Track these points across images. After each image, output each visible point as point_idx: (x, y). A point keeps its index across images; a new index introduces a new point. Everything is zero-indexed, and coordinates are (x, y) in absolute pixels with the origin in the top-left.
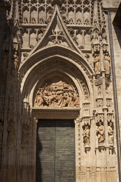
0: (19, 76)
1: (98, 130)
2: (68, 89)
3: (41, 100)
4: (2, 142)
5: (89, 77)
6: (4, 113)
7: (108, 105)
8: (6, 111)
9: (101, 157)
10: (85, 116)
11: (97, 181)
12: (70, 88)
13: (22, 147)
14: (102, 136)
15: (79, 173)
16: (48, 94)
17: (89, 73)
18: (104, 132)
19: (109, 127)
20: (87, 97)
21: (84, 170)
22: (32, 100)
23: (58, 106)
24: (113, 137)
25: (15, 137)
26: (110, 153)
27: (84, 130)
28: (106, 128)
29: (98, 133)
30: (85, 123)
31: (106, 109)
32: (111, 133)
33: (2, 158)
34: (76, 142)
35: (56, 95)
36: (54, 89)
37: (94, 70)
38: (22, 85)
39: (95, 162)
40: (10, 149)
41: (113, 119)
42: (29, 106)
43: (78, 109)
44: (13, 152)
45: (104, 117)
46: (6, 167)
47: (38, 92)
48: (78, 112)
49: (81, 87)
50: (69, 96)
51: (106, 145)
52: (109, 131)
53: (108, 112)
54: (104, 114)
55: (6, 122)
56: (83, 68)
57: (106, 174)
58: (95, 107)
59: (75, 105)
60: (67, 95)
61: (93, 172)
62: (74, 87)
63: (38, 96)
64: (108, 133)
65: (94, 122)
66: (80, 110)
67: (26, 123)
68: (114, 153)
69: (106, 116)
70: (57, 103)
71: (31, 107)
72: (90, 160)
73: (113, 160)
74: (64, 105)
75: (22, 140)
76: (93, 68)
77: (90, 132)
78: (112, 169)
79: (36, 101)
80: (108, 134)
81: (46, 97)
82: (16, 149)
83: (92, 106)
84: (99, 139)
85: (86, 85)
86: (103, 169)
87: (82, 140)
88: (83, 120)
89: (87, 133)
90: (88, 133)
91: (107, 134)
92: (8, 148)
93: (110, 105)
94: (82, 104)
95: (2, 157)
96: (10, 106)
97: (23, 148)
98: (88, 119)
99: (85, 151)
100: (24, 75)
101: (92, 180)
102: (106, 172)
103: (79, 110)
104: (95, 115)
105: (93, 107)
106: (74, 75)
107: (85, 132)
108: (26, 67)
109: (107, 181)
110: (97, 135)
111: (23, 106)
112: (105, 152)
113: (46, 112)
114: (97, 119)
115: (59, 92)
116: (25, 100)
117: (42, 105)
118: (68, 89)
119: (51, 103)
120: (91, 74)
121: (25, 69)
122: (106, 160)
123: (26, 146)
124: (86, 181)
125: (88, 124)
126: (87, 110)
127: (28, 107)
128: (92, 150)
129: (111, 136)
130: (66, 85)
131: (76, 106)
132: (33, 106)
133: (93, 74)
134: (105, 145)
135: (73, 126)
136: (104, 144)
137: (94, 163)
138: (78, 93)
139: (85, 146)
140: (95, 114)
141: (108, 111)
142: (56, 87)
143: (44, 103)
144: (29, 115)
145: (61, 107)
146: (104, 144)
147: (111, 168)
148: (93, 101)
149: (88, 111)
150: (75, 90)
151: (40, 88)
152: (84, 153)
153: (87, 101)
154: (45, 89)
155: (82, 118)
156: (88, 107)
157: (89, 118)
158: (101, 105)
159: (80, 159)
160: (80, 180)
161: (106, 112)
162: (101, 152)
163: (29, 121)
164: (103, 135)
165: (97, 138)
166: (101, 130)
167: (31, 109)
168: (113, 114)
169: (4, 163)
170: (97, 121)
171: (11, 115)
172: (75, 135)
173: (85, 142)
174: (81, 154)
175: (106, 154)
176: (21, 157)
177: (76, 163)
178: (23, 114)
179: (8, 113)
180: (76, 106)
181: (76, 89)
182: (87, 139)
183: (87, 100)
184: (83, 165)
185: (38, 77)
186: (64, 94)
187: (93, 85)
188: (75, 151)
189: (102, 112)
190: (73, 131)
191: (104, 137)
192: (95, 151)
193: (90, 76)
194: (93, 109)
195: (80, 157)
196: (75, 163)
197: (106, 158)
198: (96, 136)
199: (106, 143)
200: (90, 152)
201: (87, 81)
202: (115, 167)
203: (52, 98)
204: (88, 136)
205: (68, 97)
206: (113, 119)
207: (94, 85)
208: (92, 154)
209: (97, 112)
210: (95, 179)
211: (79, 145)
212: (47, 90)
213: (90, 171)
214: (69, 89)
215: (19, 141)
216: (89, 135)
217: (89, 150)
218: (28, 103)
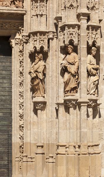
1: (64, 62)
7: (90, 6)
9: (69, 123)
10: (35, 29)
11: (59, 175)
14: (72, 78)
15: (19, 159)
18: (78, 68)
19: (90, 57)
21: (30, 151)
24: (98, 80)
26: (88, 116)
27: (34, 63)
28: (82, 59)
29: (64, 70)
30: (35, 47)
31: (84, 15)
32: (94, 72)
34: (13, 90)
39: (55, 135)
41: (99, 39)
43: (19, 11)
45: (79, 35)
48: (20, 18)
51: (81, 98)
52: (90, 67)
53: (89, 23)
54: (79, 27)
57: (79, 159)
58: (60, 9)
61: (51, 155)
64: (87, 71)
65: (56, 45)
66: (24, 14)
68: (98, 116)
69: (83, 32)
72: (45, 130)
73: (94, 131)
77: (47, 67)
78: (91, 150)
80: (86, 73)
83: (53, 8)
84: (66, 84)
86: (72, 149)
87: (28, 85)
88: (31, 40)
89: (39, 70)
90: (41, 69)
91: (83, 73)
93: (94, 7)
98: (43, 37)
99: (33, 111)
101: (48, 172)
102: (79, 155)
103: (23, 15)
104: (59, 29)
105: (55, 10)
107: (36, 67)
109: (79, 175)
110: (62, 74)
112: (78, 112)
114: (64, 38)
122: (78, 131)
124: (35, 175)
125: (42, 48)
126: (42, 15)
128: (51, 108)
129: (93, 79)
131: (14, 4)
134: (78, 98)
135: (8, 52)
136: (76, 94)
137: (54, 136)
139: (35, 100)
140: (60, 25)
141: (88, 20)
146: (76, 96)
147: (89, 146)
149: (43, 19)
152: (33, 113)
155: (30, 34)
156: (44, 8)
157: (44, 35)
158: (75, 5)
159: (21, 127)
160: (22, 174)
161: (84, 23)
162: (69, 113)
164: (76, 75)
165: (62, 80)
166: (70, 64)
168: (100, 27)
170: (64, 42)
172: (13, 74)
173: (34, 90)
174: (25, 117)
175: (81, 118)
177: (13, 138)
180: (14, 4)
182: (38, 84)
184: (29, 140)
188: (11, 109)
189: (75, 22)
190: (8, 64)
191: (78, 79)
192: (57, 111)
194: (55, 14)
195: (21, 123)
196: (10, 136)
197: (80, 125)
198: (61, 77)
199: (80, 94)
200: (45, 112)
202: (98, 145)
204: (41, 76)
206: (99, 39)
208: (50, 116)
209: (63, 20)
210: (55, 171)
211: (21, 96)
213: (43, 154)
216: (44, 75)
217: (43, 109)
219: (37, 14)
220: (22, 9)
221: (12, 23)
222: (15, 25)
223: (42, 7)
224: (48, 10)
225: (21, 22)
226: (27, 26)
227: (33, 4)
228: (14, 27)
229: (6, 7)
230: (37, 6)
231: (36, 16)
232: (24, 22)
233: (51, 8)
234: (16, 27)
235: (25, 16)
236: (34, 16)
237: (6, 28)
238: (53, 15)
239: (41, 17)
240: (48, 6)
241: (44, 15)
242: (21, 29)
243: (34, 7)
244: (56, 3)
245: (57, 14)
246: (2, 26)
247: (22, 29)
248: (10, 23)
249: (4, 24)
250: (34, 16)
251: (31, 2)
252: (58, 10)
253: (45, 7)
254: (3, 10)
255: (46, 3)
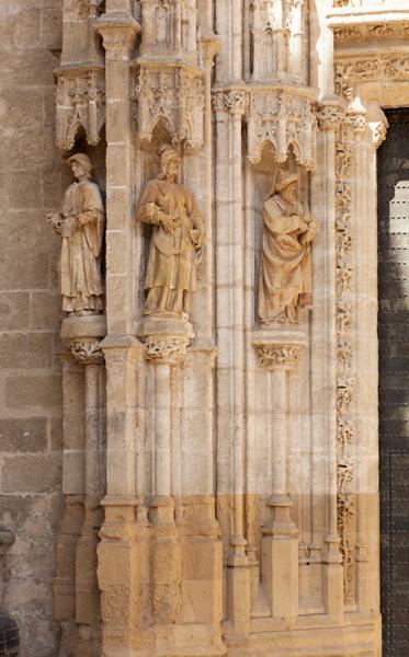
4: (102, 312)
6: (102, 73)
8: (118, 53)
13: (259, 349)
25: (200, 270)
33: (105, 443)
40: (164, 371)
44: (189, 393)
46: (143, 514)
55: (120, 151)
67: (284, 150)
75: (260, 288)
82: (216, 370)
92: (151, 360)
95: (110, 436)
96: (148, 12)
97: (265, 355)
123: (296, 336)
144: (309, 82)
163: (309, 129)
169: (125, 478)
171: (156, 91)
176: (256, 427)
179: (135, 71)
215: (236, 305)
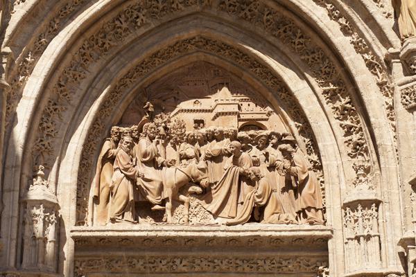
0: (9, 69)
2: (261, 127)
3: (125, 190)
5: (370, 66)
12: (276, 124)
16: (160, 160)
17: (371, 48)
20: (367, 171)
22: (74, 187)
23: (213, 221)
35: (202, 164)
36: (190, 131)
37: (396, 28)
38: (24, 110)
42: (60, 223)
47: (107, 145)
49: (333, 116)
50: (272, 168)
56: (336, 19)
59: (302, 213)
60: (256, 163)
62: (295, 119)
63: (107, 165)
66: (329, 237)
70: (209, 201)
71: (70, 226)
74: (245, 211)
76: (392, 21)
79: (93, 192)
81: (150, 172)
83: (393, 220)
85: (358, 106)
94: (338, 206)
100: (33, 64)
103: (325, 240)
105: (398, 223)
106: (296, 59)
108: (46, 22)
111: (24, 220)
113: (148, 254)
115: (214, 147)
116: (37, 191)
117: (128, 215)
118: (261, 127)
119: (176, 203)
120: (382, 52)
121: (37, 33)
126: (368, 238)
127: (51, 229)
130: (251, 110)
131: (305, 216)
132: (80, 221)
133: (391, 50)
138: (314, 147)
142: (199, 123)
143: (140, 206)
145: (229, 225)
148: (395, 190)
149: (374, 242)
150: (302, 132)
151: (115, 128)
153: (364, 192)
154: (140, 130)
167: (68, 235)
178: (24, 265)
180: (305, 216)
181: (307, 130)
183: (364, 186)
185: (104, 69)
186: (244, 155)
187: (391, 108)
193: (378, 58)
201: (360, 85)
203: (180, 176)
205: (263, 169)
207: (400, 108)
212: (151, 139)
214: (267, 132)
218: (52, 208)
219: (358, 234)
220: (323, 227)
221: (302, 258)
222: (309, 264)
223: (369, 220)
224: (381, 224)
225: (323, 256)
226: (337, 265)
227: (348, 213)
228: (308, 268)
229: (288, 224)
230: (356, 218)
231: (356, 241)
232: (330, 255)
233: (388, 220)
234: (312, 267)
235: (330, 242)
236: (352, 239)
237: (290, 270)
238: (395, 235)
239: (367, 241)
240: (380, 217)
241: (375, 236)
242: (323, 271)
243: (350, 221)
244: (398, 209)
245: (404, 231)
246: (280, 267)
247: (326, 270)
248: (298, 260)
249: (283, 262)
250: (350, 241)
251: (343, 211)
252: (406, 224)
253: (376, 220)
254: (280, 231)
255: (377, 211)
